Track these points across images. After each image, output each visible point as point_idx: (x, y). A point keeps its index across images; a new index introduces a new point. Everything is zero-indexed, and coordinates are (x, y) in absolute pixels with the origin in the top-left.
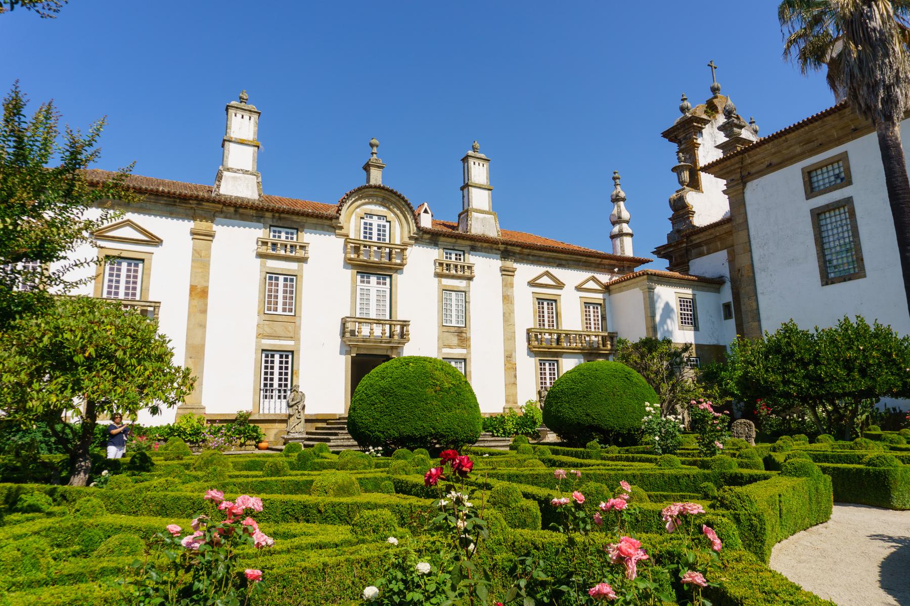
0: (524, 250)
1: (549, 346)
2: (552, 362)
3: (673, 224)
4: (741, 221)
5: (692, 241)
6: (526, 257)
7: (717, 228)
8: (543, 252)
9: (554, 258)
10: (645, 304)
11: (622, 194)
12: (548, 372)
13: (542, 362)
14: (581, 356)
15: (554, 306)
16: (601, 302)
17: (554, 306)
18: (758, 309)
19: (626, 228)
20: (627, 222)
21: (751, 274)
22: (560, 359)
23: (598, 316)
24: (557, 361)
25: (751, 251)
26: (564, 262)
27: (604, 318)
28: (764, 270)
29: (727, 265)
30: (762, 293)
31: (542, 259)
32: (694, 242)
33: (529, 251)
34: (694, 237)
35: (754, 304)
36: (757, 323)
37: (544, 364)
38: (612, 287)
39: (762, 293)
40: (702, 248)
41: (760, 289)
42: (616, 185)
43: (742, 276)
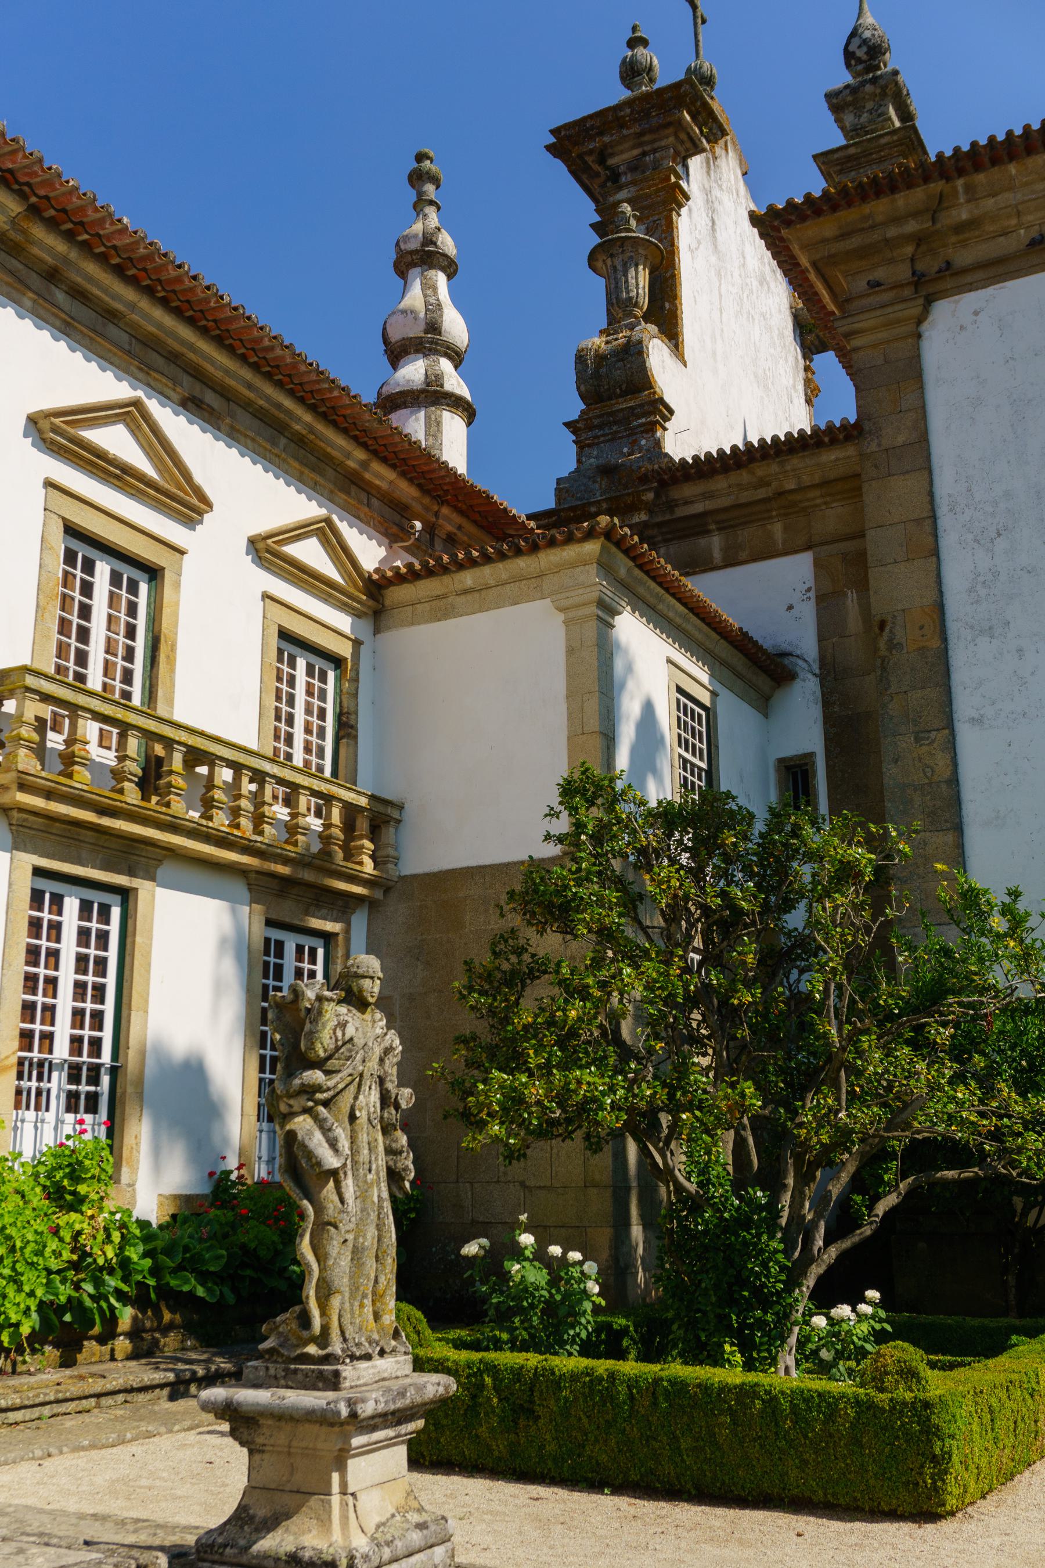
0: (38, 232)
1: (104, 791)
2: (97, 897)
3: (581, 446)
4: (901, 439)
5: (672, 505)
6: (35, 280)
7: (795, 462)
8: (129, 294)
9: (173, 358)
10: (571, 675)
11: (447, 243)
12: (69, 948)
13: (50, 887)
14: (241, 889)
15: (142, 601)
16: (345, 650)
17: (142, 601)
18: (954, 781)
19: (454, 383)
20: (457, 357)
21: (935, 643)
22: (144, 888)
23: (322, 714)
24: (126, 895)
25: (936, 553)
26: (210, 398)
27: (346, 728)
28: (989, 632)
29: (808, 611)
30: (977, 721)
31: (113, 331)
32: (681, 512)
33: (61, 246)
34: (688, 490)
35: (941, 760)
36: (950, 838)
37: (57, 901)
38: (398, 594)
39: (973, 720)
40: (702, 542)
41: (965, 704)
42: (420, 204)
43: (892, 646)
